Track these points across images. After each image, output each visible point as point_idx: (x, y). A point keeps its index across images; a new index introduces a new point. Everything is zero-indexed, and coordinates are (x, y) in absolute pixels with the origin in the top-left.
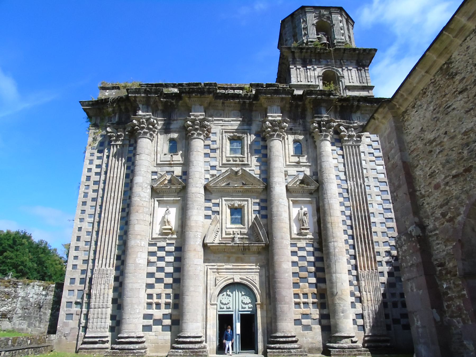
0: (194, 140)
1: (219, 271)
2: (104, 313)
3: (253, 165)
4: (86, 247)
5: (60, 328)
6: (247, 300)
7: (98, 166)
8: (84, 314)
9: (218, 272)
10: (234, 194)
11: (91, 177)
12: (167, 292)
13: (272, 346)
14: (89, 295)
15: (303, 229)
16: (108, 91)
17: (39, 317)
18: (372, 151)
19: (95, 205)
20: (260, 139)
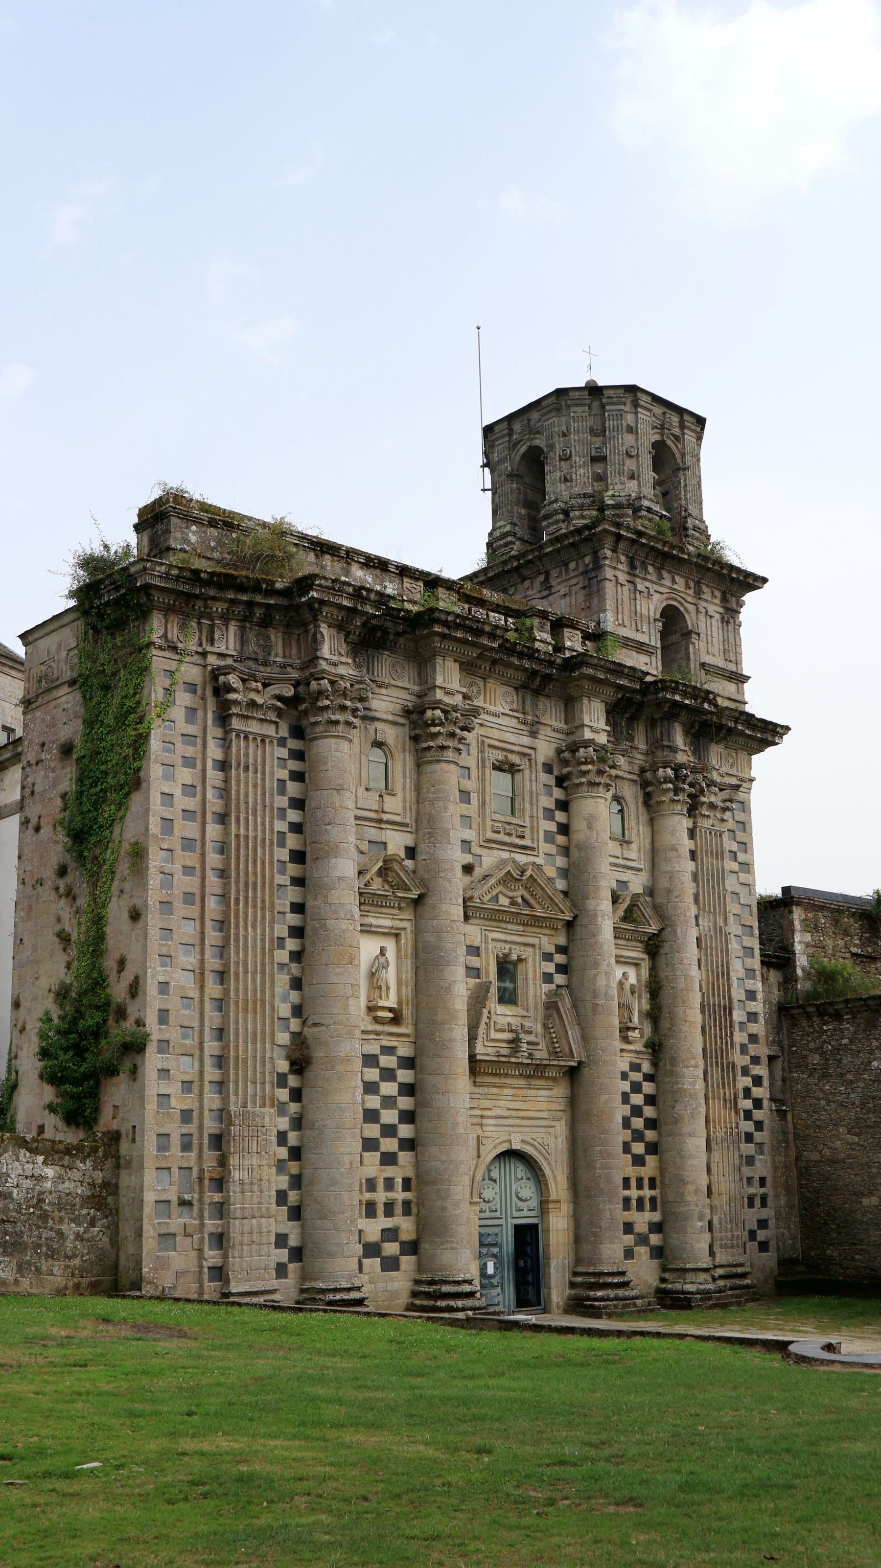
0: (445, 766)
1: (485, 1121)
2: (265, 1230)
3: (541, 854)
4: (188, 1042)
5: (149, 1273)
6: (528, 1190)
7: (189, 789)
8: (211, 1235)
9: (481, 1125)
10: (510, 926)
11: (175, 823)
12: (389, 1175)
13: (600, 1294)
14: (220, 1184)
15: (628, 1029)
16: (194, 528)
17: (47, 1244)
18: (734, 847)
19: (196, 914)
20: (551, 780)
